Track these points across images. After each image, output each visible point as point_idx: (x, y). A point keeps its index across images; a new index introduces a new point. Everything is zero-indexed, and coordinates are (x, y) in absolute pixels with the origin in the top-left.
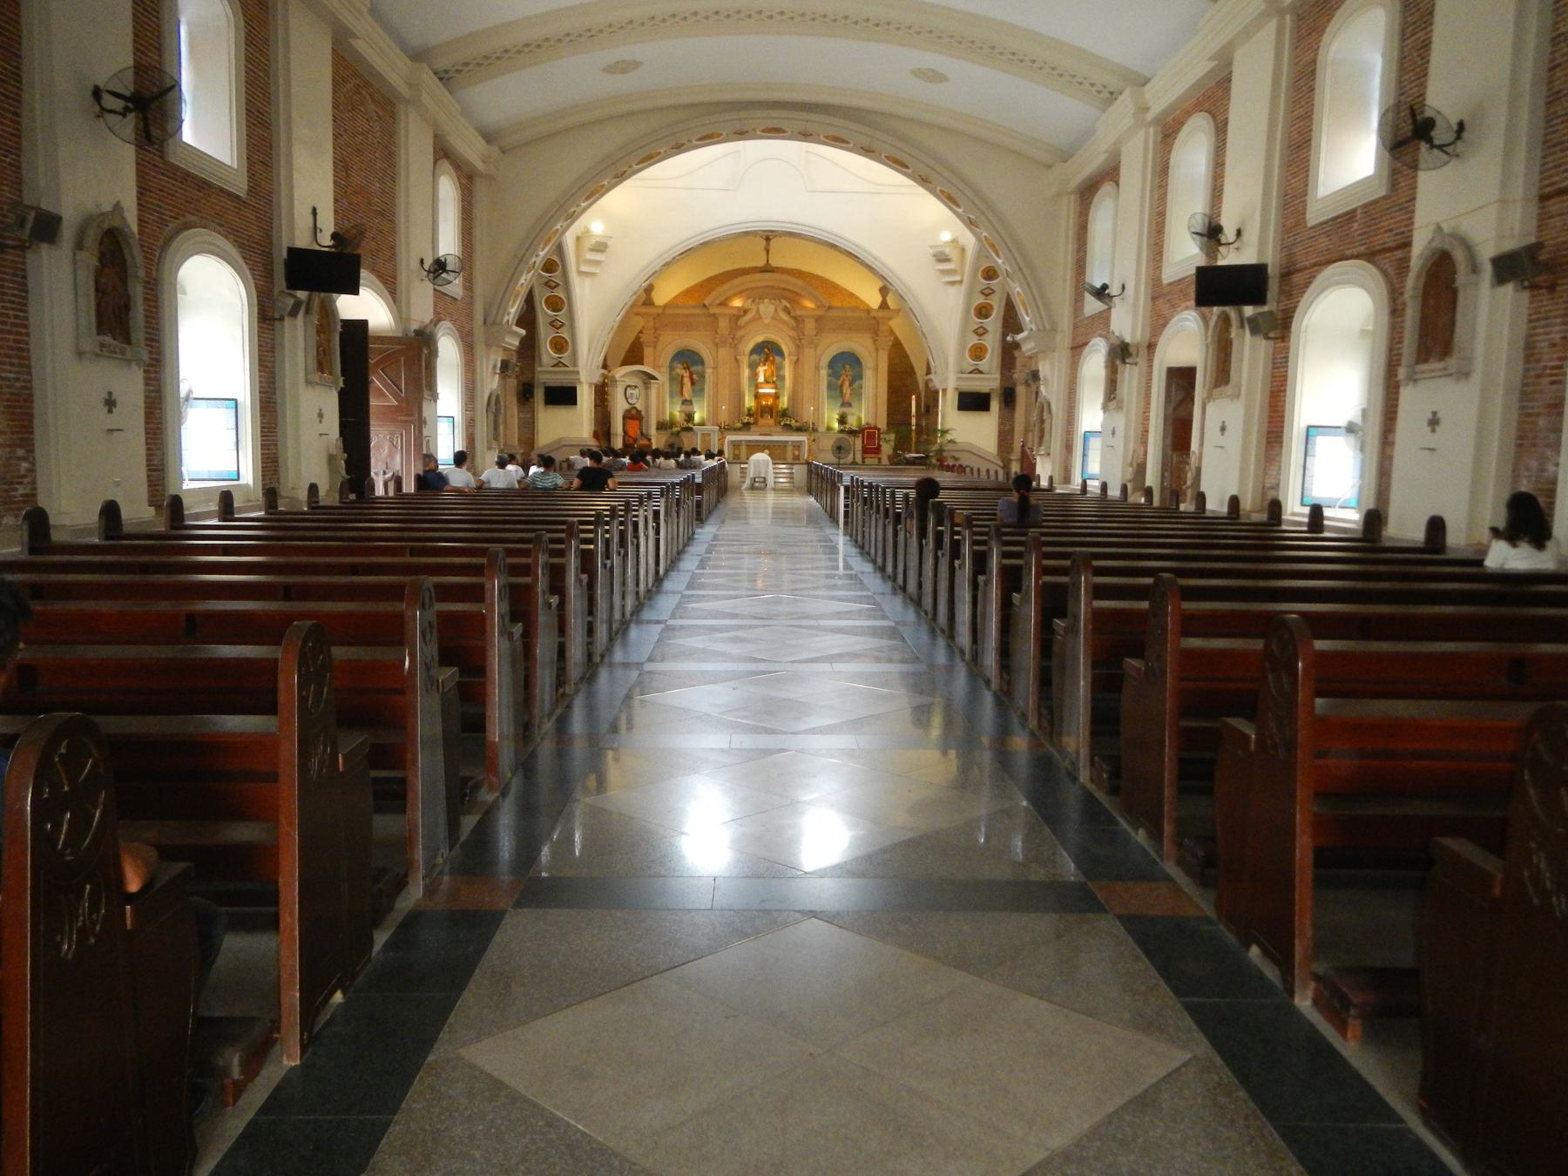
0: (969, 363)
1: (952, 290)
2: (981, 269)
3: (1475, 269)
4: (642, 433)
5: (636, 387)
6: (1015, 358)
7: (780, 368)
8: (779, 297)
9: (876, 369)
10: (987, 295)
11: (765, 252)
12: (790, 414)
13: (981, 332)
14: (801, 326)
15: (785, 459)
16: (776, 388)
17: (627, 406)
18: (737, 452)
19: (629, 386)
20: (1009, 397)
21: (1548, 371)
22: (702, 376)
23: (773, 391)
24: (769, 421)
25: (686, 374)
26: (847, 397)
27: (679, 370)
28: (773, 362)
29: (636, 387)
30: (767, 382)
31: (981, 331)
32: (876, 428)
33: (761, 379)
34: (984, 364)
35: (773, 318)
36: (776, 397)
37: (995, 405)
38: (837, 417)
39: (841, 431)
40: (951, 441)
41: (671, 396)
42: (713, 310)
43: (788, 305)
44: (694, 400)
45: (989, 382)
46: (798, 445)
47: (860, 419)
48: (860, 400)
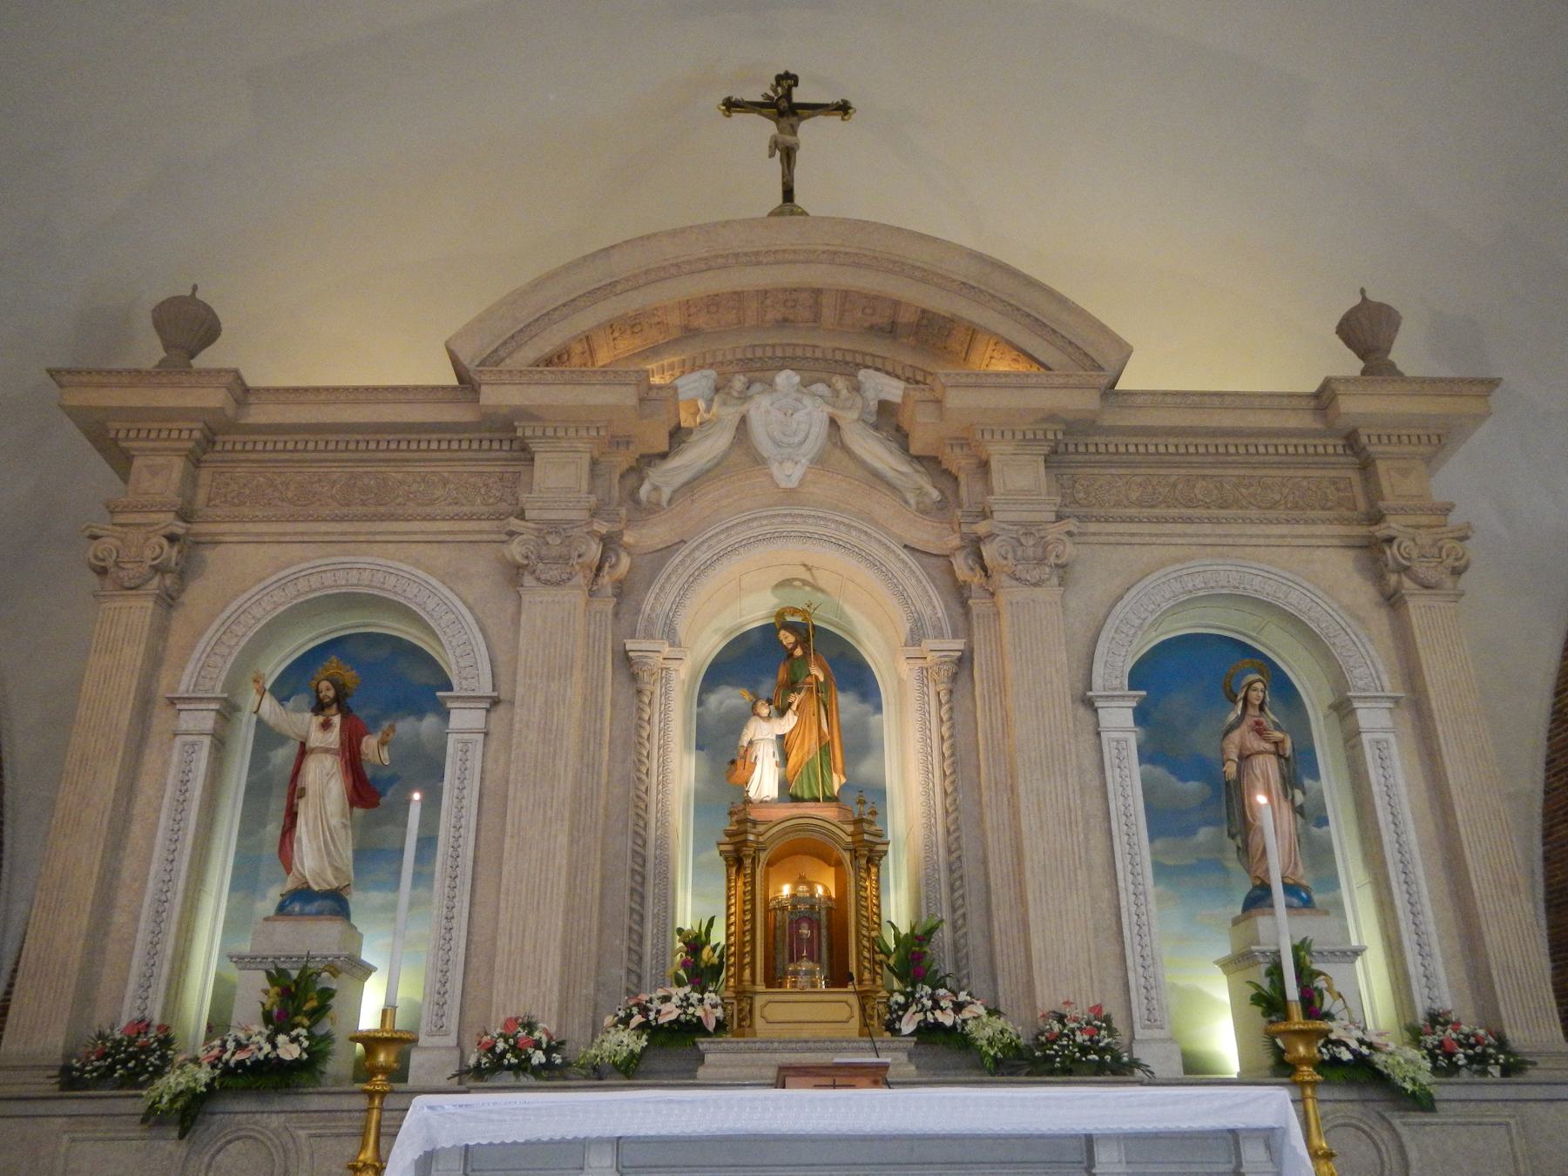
7: (862, 745)
11: (776, 164)
14: (969, 489)
33: (764, 782)
35: (819, 461)
41: (245, 880)
42: (498, 396)
43: (893, 390)
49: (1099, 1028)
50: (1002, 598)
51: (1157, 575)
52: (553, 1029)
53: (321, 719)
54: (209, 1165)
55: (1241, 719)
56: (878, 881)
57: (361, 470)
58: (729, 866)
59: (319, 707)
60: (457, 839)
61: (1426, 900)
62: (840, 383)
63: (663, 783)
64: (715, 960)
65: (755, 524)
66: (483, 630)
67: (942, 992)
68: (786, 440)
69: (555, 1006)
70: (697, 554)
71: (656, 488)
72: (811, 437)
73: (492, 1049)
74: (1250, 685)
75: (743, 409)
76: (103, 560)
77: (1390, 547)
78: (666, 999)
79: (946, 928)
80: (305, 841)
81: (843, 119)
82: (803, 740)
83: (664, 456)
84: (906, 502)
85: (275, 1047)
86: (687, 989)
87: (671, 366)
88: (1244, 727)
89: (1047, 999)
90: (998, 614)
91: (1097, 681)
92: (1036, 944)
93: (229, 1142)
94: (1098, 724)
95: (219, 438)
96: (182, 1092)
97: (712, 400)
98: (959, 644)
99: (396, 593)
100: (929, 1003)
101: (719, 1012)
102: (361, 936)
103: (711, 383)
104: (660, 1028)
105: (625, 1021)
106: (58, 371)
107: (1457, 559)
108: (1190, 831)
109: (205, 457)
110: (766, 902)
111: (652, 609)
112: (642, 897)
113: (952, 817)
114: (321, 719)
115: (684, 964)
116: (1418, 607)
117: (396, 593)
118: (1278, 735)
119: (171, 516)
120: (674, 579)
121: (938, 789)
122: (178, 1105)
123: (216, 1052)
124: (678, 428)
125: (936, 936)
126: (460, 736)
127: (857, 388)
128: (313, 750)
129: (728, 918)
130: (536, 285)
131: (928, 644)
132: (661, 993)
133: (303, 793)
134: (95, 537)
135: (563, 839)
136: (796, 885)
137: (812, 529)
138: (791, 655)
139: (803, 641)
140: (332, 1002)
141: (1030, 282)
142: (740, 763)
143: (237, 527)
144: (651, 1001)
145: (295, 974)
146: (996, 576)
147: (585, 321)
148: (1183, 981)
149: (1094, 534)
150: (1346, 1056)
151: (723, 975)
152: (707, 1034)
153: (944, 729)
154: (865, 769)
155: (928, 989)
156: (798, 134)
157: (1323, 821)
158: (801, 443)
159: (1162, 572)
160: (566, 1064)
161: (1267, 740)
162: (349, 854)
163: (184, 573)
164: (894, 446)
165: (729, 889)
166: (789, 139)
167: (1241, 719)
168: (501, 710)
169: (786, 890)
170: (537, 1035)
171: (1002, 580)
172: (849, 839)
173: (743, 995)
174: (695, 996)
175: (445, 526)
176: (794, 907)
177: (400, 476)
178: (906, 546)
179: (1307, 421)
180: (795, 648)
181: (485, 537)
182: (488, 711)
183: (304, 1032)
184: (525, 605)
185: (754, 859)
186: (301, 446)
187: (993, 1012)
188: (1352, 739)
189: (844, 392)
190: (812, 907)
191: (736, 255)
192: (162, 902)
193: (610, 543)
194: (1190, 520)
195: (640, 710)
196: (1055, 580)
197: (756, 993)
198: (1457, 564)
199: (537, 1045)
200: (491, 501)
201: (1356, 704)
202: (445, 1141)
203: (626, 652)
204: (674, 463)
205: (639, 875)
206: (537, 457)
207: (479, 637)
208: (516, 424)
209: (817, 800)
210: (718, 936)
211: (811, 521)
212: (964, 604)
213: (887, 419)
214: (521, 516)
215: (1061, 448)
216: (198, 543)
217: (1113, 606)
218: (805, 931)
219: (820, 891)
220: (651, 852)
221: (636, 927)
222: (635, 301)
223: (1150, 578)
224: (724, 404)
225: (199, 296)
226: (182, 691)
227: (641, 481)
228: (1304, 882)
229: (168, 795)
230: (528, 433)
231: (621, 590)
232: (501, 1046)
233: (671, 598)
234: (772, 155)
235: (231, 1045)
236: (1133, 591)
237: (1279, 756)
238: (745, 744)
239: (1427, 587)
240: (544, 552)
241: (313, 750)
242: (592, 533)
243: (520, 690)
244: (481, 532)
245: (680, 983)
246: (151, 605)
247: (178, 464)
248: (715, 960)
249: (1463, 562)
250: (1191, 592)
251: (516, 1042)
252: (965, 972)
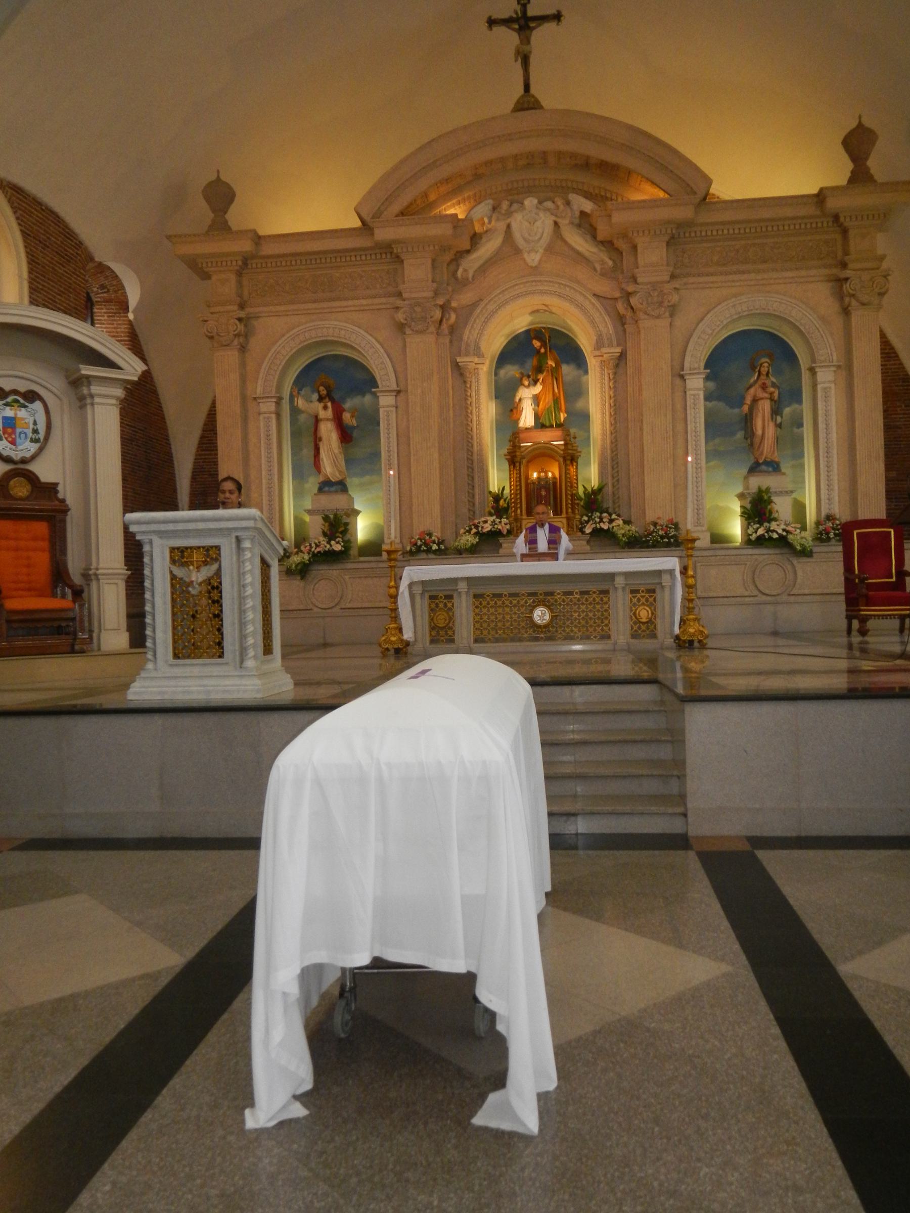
5: (31, 396)
7: (577, 392)
8: (562, 190)
9: (847, 367)
11: (518, 67)
12: (608, 504)
18: (441, 621)
22: (372, 420)
25: (326, 414)
26: (767, 449)
27: (309, 404)
28: (555, 373)
30: (540, 425)
33: (527, 419)
36: (570, 457)
38: (736, 507)
41: (299, 475)
42: (383, 234)
43: (588, 206)
44: (352, 482)
47: (799, 508)
48: (799, 455)
49: (670, 528)
50: (641, 324)
51: (723, 304)
52: (439, 535)
53: (322, 405)
54: (313, 589)
55: (756, 382)
56: (577, 468)
57: (319, 272)
58: (510, 465)
59: (321, 399)
60: (389, 456)
61: (835, 466)
62: (560, 202)
63: (479, 425)
64: (506, 505)
65: (517, 287)
66: (388, 356)
67: (605, 515)
68: (531, 238)
69: (439, 526)
70: (488, 307)
71: (465, 270)
72: (545, 235)
73: (416, 544)
74: (761, 365)
75: (508, 221)
76: (210, 333)
77: (846, 283)
78: (486, 522)
79: (610, 485)
80: (325, 460)
81: (558, 24)
82: (545, 398)
83: (468, 252)
84: (595, 270)
85: (331, 546)
86: (494, 517)
87: (469, 197)
88: (757, 386)
89: (650, 516)
90: (639, 332)
91: (687, 365)
92: (647, 493)
93: (320, 580)
94: (685, 387)
95: (248, 262)
96: (299, 564)
97: (491, 216)
98: (619, 350)
99: (346, 339)
100: (598, 520)
101: (508, 527)
102: (353, 498)
103: (490, 207)
104: (483, 534)
105: (469, 531)
106: (170, 236)
107: (881, 288)
108: (733, 434)
109: (244, 272)
110: (527, 478)
111: (468, 338)
112: (473, 478)
113: (614, 435)
114: (322, 405)
115: (493, 507)
116: (855, 318)
117: (346, 339)
118: (772, 389)
119: (235, 308)
120: (477, 321)
121: (608, 421)
122: (299, 567)
123: (308, 548)
124: (475, 234)
125: (604, 490)
126: (385, 409)
127: (568, 203)
128: (321, 420)
129: (510, 487)
130: (396, 168)
131: (604, 350)
132: (483, 519)
133: (320, 439)
134: (206, 321)
135: (436, 455)
136: (539, 473)
137: (546, 288)
138: (538, 352)
139: (544, 344)
140: (349, 527)
141: (659, 142)
142: (514, 411)
143: (266, 309)
144: (479, 523)
145: (332, 516)
146: (638, 313)
147: (423, 184)
148: (721, 504)
149: (692, 283)
150: (775, 536)
151: (510, 511)
152: (503, 536)
153: (611, 393)
154: (580, 404)
155: (598, 514)
156: (532, 42)
157: (801, 425)
158: (540, 239)
159: (725, 303)
160: (446, 549)
161: (766, 392)
162: (343, 462)
163: (246, 336)
164: (588, 237)
165: (510, 475)
166: (526, 48)
167: (756, 382)
168: (402, 394)
169: (535, 475)
170: (433, 538)
171: (642, 315)
172: (562, 452)
173: (516, 520)
174: (498, 520)
175: (364, 302)
176: (539, 483)
177: (337, 275)
178: (594, 295)
179: (811, 210)
180: (541, 348)
181: (384, 306)
182: (396, 396)
183: (341, 540)
184: (408, 344)
185: (520, 463)
186: (289, 263)
187: (627, 522)
188: (814, 386)
189: (562, 207)
190: (547, 482)
191: (499, 137)
192: (269, 488)
193: (444, 308)
194: (743, 272)
195: (466, 391)
196: (667, 314)
197: (522, 519)
198: (881, 291)
199: (434, 542)
200: (384, 286)
201: (817, 370)
202: (416, 579)
203: (457, 363)
204: (474, 256)
205: (471, 468)
206: (405, 262)
207: (388, 360)
208: (393, 246)
209: (552, 426)
211: (545, 284)
212: (623, 324)
213: (585, 222)
214: (400, 294)
215: (676, 236)
216: (250, 318)
217: (698, 324)
218: (543, 493)
219: (550, 475)
220: (475, 457)
221: (471, 491)
222: (447, 170)
223: (720, 307)
224: (498, 220)
225: (223, 178)
226: (258, 396)
227: (458, 266)
228: (777, 459)
229: (262, 442)
230: (399, 250)
231: (452, 330)
232: (419, 543)
233: (477, 331)
234: (516, 60)
235: (313, 545)
236: (709, 316)
237: (771, 399)
238: (517, 401)
239: (863, 304)
240: (414, 315)
241: (321, 420)
242: (435, 305)
243: (410, 387)
244: (381, 304)
245: (491, 514)
246: (236, 353)
247: (233, 277)
248: (506, 505)
249: (883, 290)
250: (740, 313)
251: (425, 540)
252: (617, 505)
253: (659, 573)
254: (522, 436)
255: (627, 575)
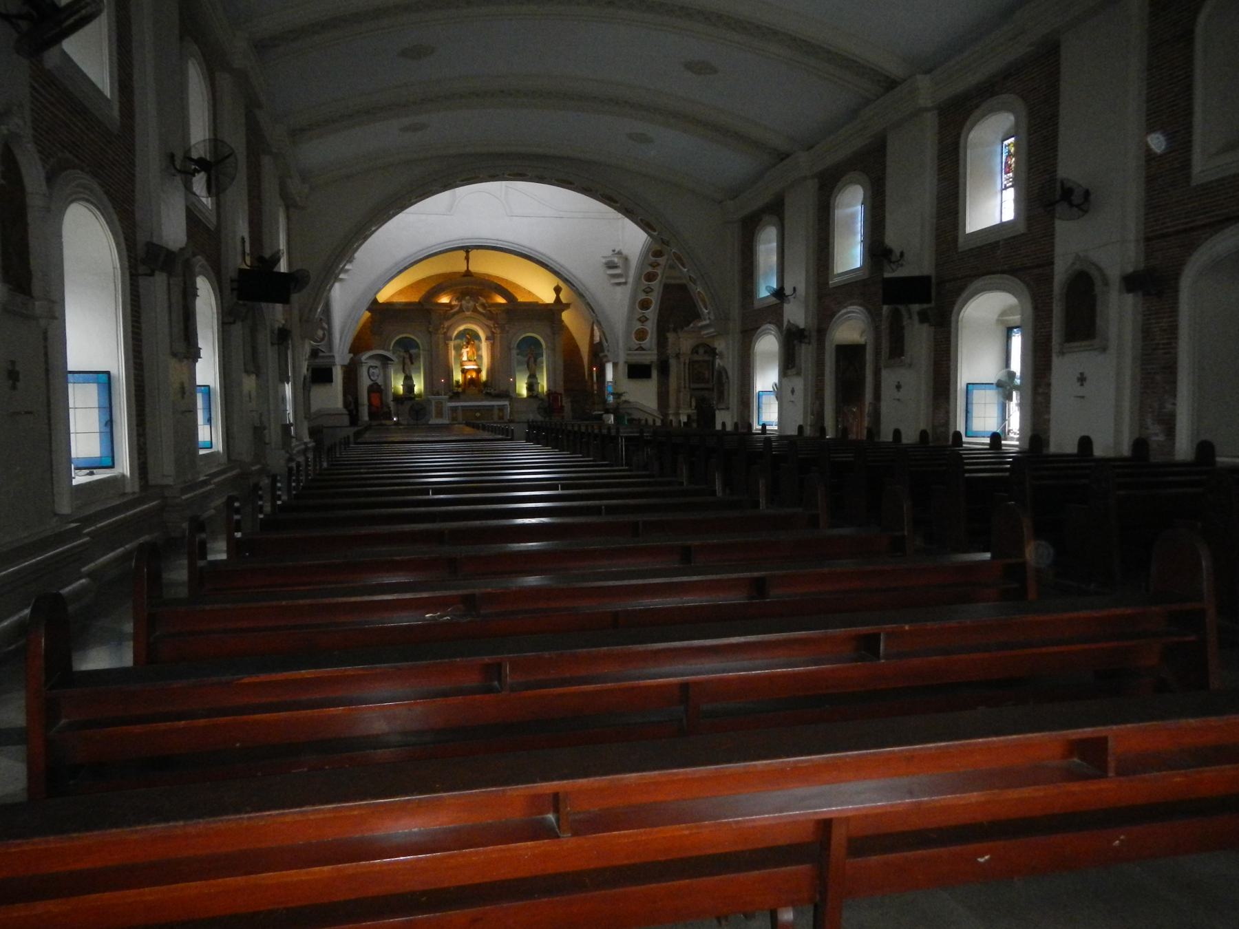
0: (635, 343)
1: (619, 289)
2: (646, 272)
3: (1106, 283)
4: (382, 403)
5: (376, 367)
6: (667, 339)
7: (478, 349)
10: (647, 293)
11: (466, 261)
13: (643, 320)
15: (492, 419)
16: (477, 365)
17: (371, 383)
19: (371, 367)
20: (664, 369)
21: (1161, 346)
23: (475, 367)
24: (473, 390)
25: (407, 356)
29: (376, 367)
31: (643, 319)
32: (555, 393)
33: (465, 358)
34: (647, 343)
36: (479, 371)
37: (654, 374)
39: (529, 396)
40: (626, 402)
45: (650, 357)
46: (501, 409)
154: (480, 353)
169: (469, 377)
187: (495, 390)
205: (449, 374)
210: (461, 381)
253: (504, 405)
254: (464, 363)
255: (498, 406)
